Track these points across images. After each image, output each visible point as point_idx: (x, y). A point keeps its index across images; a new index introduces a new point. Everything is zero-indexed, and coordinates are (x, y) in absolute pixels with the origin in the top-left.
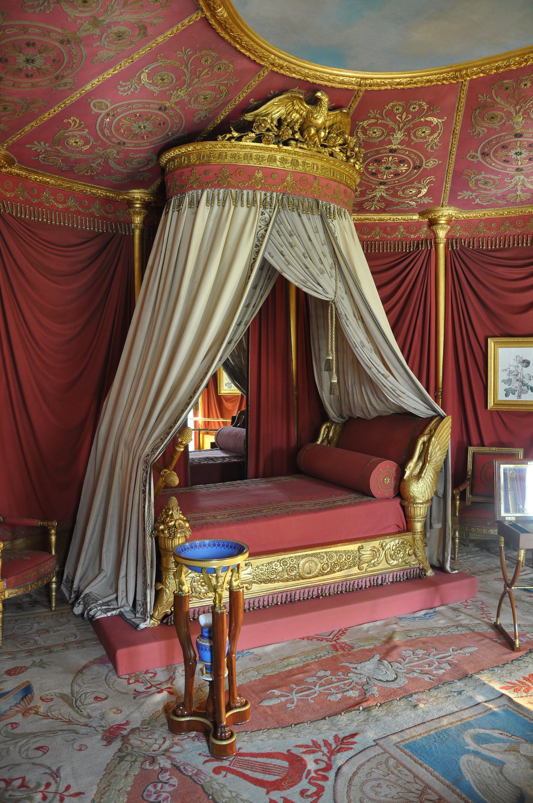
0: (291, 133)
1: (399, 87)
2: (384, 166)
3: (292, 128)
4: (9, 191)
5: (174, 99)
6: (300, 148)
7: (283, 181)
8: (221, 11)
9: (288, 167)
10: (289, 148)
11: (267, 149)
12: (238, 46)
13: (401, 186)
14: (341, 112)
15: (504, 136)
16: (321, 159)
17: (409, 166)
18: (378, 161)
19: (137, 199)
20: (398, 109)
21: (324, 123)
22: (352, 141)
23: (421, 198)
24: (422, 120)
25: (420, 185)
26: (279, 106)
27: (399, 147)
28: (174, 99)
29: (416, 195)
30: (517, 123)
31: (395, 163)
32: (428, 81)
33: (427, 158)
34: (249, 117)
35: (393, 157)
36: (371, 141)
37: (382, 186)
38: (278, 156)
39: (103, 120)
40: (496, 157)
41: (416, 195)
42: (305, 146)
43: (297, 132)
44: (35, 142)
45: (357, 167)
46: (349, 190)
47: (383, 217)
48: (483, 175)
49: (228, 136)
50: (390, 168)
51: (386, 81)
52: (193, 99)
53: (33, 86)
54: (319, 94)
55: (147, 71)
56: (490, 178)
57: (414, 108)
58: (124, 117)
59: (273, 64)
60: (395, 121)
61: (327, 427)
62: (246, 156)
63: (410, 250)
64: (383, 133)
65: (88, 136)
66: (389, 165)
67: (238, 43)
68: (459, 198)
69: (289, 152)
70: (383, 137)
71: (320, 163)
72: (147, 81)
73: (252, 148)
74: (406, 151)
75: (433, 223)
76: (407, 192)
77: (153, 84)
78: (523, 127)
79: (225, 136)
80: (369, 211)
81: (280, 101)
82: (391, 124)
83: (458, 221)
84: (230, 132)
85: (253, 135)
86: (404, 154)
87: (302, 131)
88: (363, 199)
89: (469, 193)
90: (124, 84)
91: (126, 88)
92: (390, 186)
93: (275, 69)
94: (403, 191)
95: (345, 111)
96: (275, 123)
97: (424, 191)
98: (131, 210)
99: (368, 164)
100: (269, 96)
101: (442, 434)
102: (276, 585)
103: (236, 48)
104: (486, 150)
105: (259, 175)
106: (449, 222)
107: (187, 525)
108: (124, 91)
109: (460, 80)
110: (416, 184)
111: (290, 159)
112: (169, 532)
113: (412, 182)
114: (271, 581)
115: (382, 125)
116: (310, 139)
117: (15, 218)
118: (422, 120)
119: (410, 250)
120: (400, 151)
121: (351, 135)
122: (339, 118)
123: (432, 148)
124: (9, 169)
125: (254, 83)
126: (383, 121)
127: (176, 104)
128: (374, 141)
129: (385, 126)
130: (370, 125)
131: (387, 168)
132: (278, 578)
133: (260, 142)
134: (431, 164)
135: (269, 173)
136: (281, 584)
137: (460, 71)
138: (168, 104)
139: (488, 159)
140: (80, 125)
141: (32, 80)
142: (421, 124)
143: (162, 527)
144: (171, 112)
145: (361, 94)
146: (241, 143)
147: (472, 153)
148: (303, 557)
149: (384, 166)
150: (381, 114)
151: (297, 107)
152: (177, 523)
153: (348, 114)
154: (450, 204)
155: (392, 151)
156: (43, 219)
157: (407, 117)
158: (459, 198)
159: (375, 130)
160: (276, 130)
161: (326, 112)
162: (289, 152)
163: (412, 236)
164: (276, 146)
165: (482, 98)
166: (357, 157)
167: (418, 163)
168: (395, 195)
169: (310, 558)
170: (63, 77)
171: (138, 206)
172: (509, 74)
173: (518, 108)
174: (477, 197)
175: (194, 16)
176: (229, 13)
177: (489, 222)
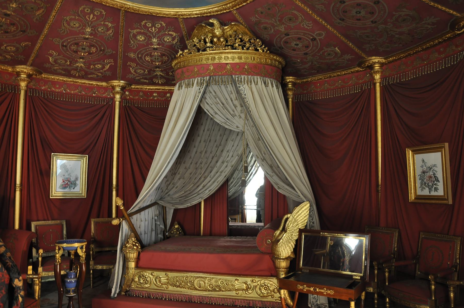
9: (210, 62)
10: (206, 52)
42: (214, 49)
43: (207, 43)
49: (179, 54)
54: (211, 21)
101: (301, 214)
111: (210, 58)
117: (138, 108)
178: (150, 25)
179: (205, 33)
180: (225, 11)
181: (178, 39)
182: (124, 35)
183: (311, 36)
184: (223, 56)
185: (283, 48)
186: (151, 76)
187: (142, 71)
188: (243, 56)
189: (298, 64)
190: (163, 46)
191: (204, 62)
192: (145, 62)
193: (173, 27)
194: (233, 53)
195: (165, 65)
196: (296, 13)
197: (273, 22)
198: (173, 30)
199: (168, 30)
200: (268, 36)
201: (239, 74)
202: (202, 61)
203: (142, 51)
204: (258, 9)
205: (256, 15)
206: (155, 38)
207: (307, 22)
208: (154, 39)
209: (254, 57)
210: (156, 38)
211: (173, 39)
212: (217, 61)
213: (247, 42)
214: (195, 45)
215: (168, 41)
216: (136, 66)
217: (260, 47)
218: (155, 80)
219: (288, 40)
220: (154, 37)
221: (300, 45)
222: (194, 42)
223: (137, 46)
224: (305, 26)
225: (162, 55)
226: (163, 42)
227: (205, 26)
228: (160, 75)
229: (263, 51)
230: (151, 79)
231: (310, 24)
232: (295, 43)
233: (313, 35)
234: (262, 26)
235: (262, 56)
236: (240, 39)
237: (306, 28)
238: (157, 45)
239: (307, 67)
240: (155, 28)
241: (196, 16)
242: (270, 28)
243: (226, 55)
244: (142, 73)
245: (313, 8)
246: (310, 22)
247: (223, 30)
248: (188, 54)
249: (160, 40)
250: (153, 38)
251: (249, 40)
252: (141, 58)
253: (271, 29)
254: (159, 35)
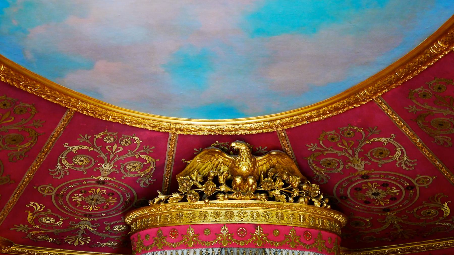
9: (222, 220)
10: (217, 201)
38: (210, 211)
42: (235, 197)
43: (222, 184)
49: (156, 200)
55: (63, 157)
69: (222, 206)
72: (69, 164)
79: (154, 201)
85: (178, 195)
86: (380, 177)
90: (53, 171)
108: (57, 176)
111: (223, 212)
120: (373, 176)
126: (328, 152)
135: (199, 229)
160: (200, 186)
162: (222, 206)
164: (202, 202)
178: (112, 139)
179: (215, 165)
180: (265, 131)
181: (152, 169)
182: (48, 153)
183: (408, 181)
184: (248, 211)
185: (347, 198)
186: (65, 231)
187: (52, 220)
188: (286, 212)
189: (365, 226)
190: (119, 177)
191: (210, 220)
192: (66, 204)
193: (153, 148)
194: (268, 206)
195: (104, 213)
196: (394, 144)
197: (347, 155)
198: (150, 153)
199: (142, 151)
200: (328, 176)
201: (277, 248)
202: (205, 216)
203: (72, 184)
204: (329, 133)
205: (321, 142)
206: (110, 163)
207: (409, 160)
208: (108, 164)
209: (304, 215)
210: (112, 163)
211: (144, 168)
212: (236, 220)
213: (295, 188)
214: (195, 187)
215: (132, 170)
216: (45, 210)
217: (316, 198)
218: (69, 240)
219: (363, 185)
220: (109, 161)
221: (381, 196)
222: (193, 180)
223: (65, 176)
224: (402, 165)
225: (110, 194)
226: (122, 170)
227: (220, 154)
228: (87, 230)
229: (322, 205)
230: (62, 236)
231: (413, 163)
232: (374, 191)
233: (412, 180)
234: (324, 160)
235: (316, 214)
236: (284, 181)
237: (404, 168)
238: (108, 176)
239: (378, 232)
240: (119, 145)
241: (206, 133)
242: (337, 165)
243: (255, 209)
244: (50, 224)
245: (426, 138)
246: (413, 159)
247: (254, 162)
248: (179, 202)
249: (119, 168)
250: (106, 162)
251: (299, 184)
252: (64, 196)
253: (339, 166)
254: (120, 158)
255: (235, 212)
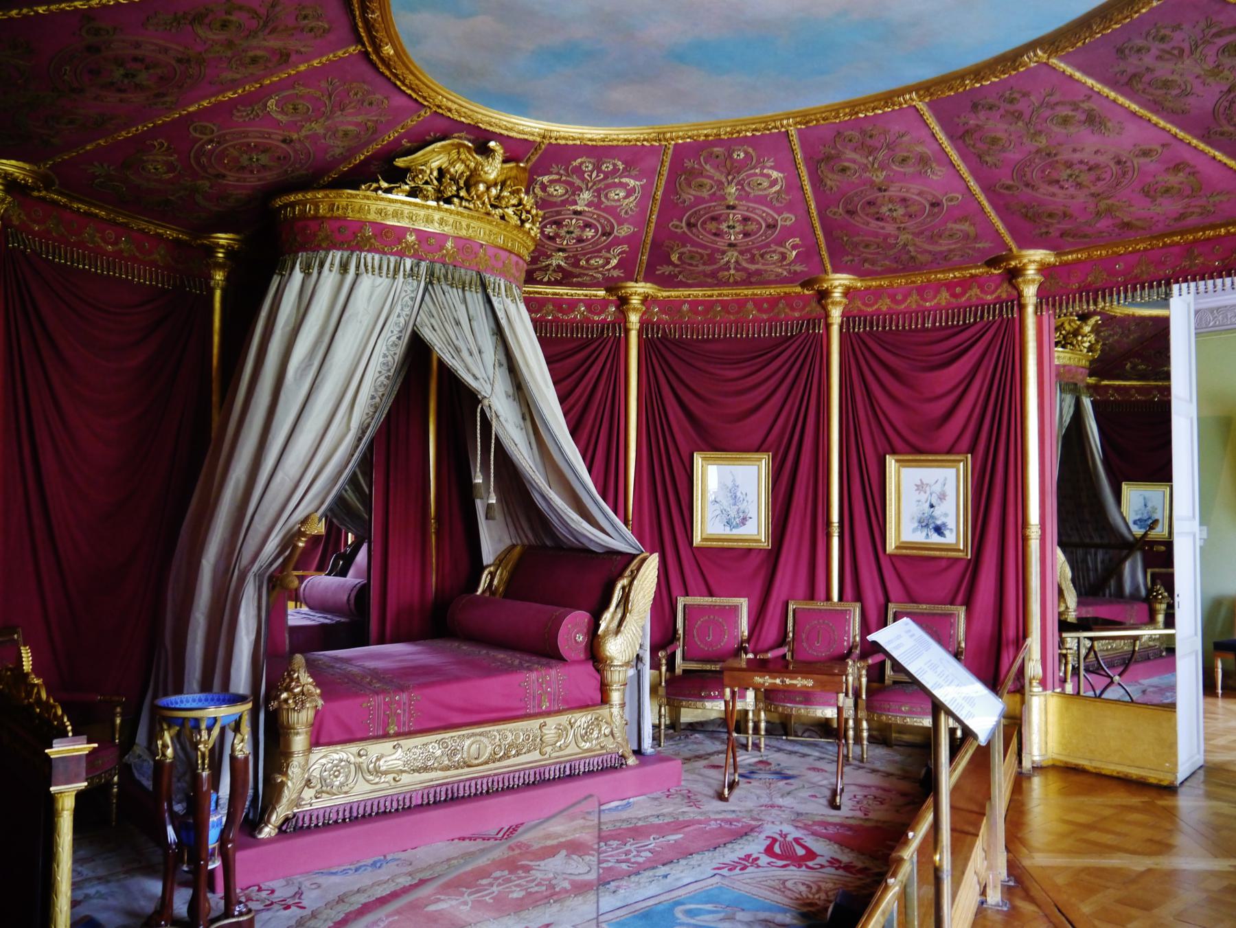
0: (455, 188)
1: (590, 143)
2: (565, 229)
3: (458, 183)
4: (38, 223)
5: (304, 133)
6: (465, 207)
7: (442, 247)
8: (388, 50)
9: (447, 230)
10: (452, 207)
11: (423, 206)
12: (399, 83)
13: (585, 255)
14: (518, 166)
15: (715, 206)
16: (490, 223)
17: (597, 231)
18: (558, 224)
19: (222, 246)
20: (587, 167)
21: (496, 179)
22: (528, 200)
23: (609, 270)
24: (616, 180)
25: (608, 255)
26: (440, 153)
27: (586, 209)
28: (304, 133)
29: (603, 266)
30: (730, 194)
31: (579, 227)
32: (625, 140)
33: (620, 224)
34: (400, 162)
35: (577, 220)
36: (551, 199)
37: (561, 254)
38: (437, 216)
39: (203, 146)
40: (705, 229)
41: (603, 266)
42: (472, 206)
44: (96, 163)
45: (533, 233)
46: (521, 262)
47: (557, 291)
48: (689, 248)
49: (375, 185)
50: (572, 233)
51: (576, 136)
52: (330, 133)
53: (121, 100)
54: (492, 144)
56: (697, 252)
57: (607, 167)
58: (233, 146)
59: (439, 107)
60: (583, 179)
61: (490, 573)
62: (396, 214)
63: (592, 336)
64: (567, 192)
65: (176, 163)
66: (572, 229)
67: (399, 80)
68: (657, 273)
69: (451, 212)
70: (567, 196)
71: (489, 227)
73: (403, 203)
74: (594, 214)
75: (623, 301)
76: (592, 262)
77: (283, 112)
78: (737, 199)
79: (370, 186)
80: (541, 283)
81: (443, 147)
82: (578, 182)
83: (655, 300)
84: (377, 181)
85: (407, 187)
87: (468, 186)
88: (534, 267)
89: (671, 268)
91: (245, 114)
92: (571, 254)
93: (440, 111)
94: (587, 261)
95: (522, 165)
96: (435, 173)
97: (614, 262)
98: (211, 261)
99: (545, 226)
100: (428, 138)
102: (433, 775)
103: (395, 85)
104: (692, 220)
105: (411, 238)
106: (645, 300)
107: (318, 691)
109: (664, 143)
110: (604, 253)
112: (295, 702)
113: (599, 251)
114: (426, 769)
115: (566, 182)
116: (478, 197)
118: (616, 180)
119: (592, 336)
121: (527, 193)
122: (514, 173)
123: (626, 212)
124: (43, 193)
125: (411, 122)
127: (307, 137)
128: (554, 199)
129: (571, 184)
130: (551, 182)
131: (568, 232)
132: (436, 765)
133: (416, 197)
134: (624, 231)
135: (423, 236)
136: (440, 774)
137: (664, 133)
138: (295, 136)
139: (694, 230)
140: (168, 148)
141: (123, 95)
142: (615, 185)
143: (284, 695)
144: (298, 146)
145: (543, 147)
146: (389, 196)
147: (675, 222)
148: (469, 737)
149: (565, 229)
150: (566, 170)
151: (463, 156)
152: (305, 689)
153: (524, 169)
154: (646, 280)
155: (576, 213)
156: (84, 265)
157: (597, 176)
158: (657, 273)
159: (557, 188)
160: (435, 182)
161: (499, 166)
162: (451, 212)
163: (596, 318)
164: (434, 204)
165: (688, 164)
166: (533, 223)
167: (608, 229)
168: (576, 264)
169: (478, 738)
170: (164, 95)
171: (221, 255)
172: (719, 141)
173: (730, 178)
174: (680, 273)
175: (351, 49)
176: (395, 51)
177: (694, 304)
212: (463, 233)
255: (464, 225)
